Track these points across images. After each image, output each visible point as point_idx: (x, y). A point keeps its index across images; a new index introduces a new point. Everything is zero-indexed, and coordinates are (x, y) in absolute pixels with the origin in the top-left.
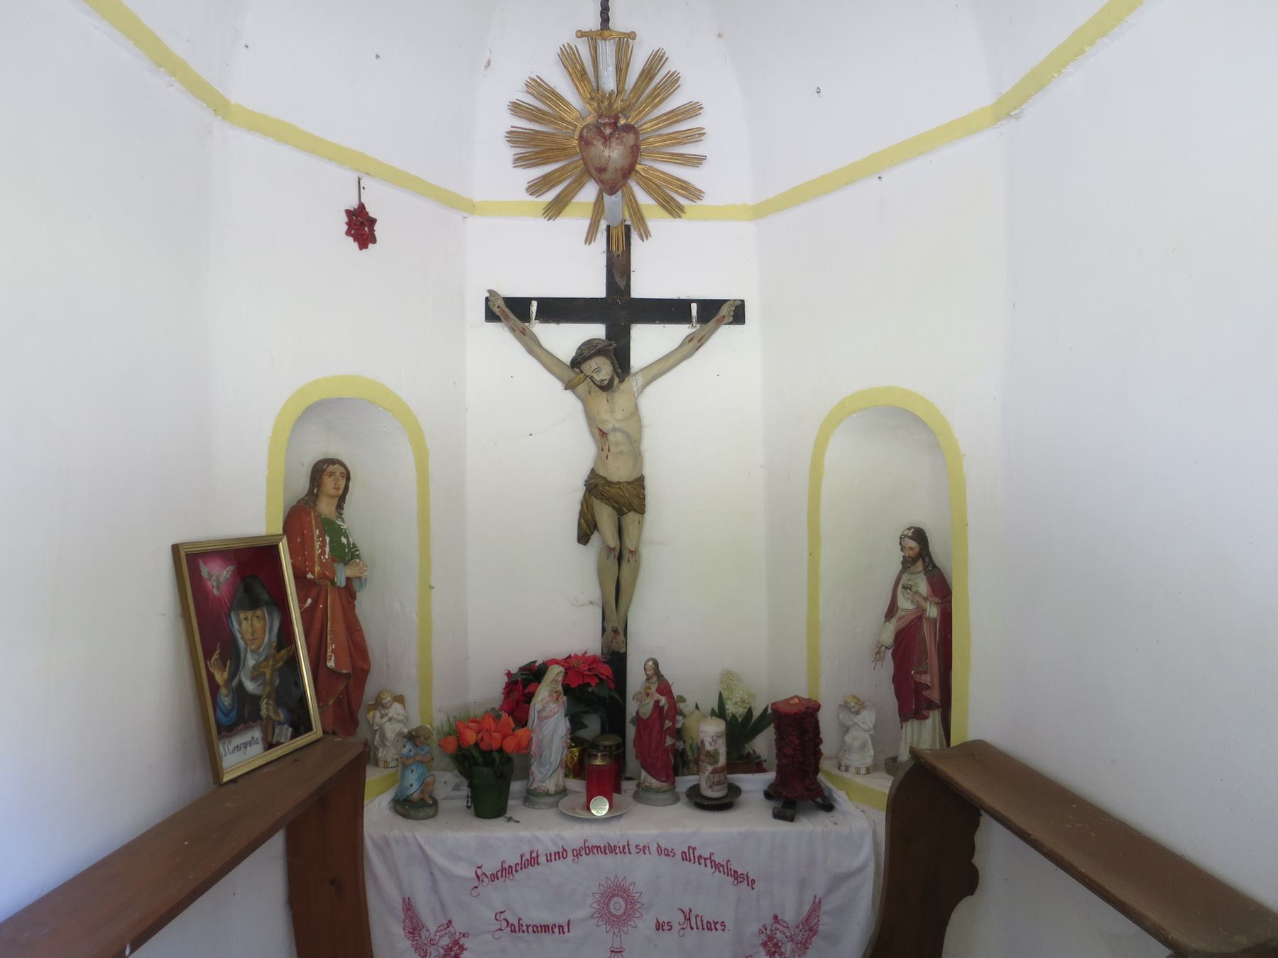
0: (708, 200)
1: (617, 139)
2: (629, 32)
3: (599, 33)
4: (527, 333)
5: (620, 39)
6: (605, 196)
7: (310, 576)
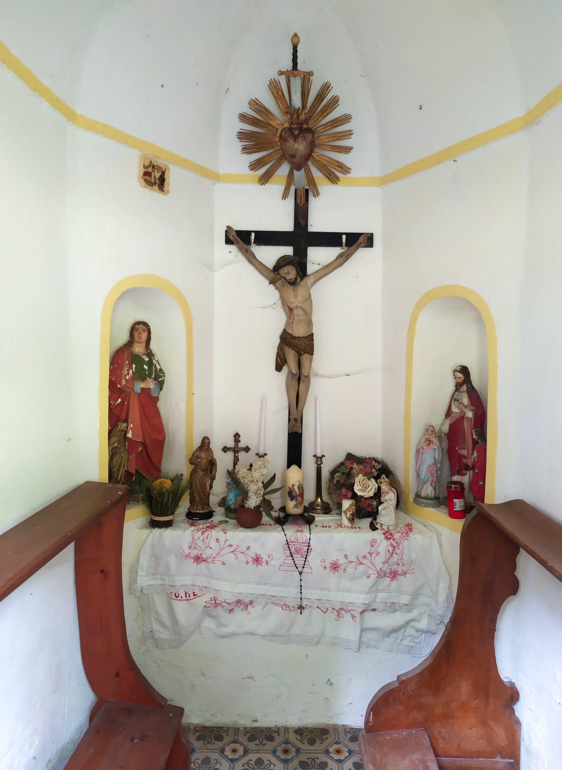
0: (353, 174)
1: (302, 137)
2: (309, 71)
3: (292, 72)
4: (248, 251)
5: (305, 76)
6: (295, 171)
7: (119, 386)
